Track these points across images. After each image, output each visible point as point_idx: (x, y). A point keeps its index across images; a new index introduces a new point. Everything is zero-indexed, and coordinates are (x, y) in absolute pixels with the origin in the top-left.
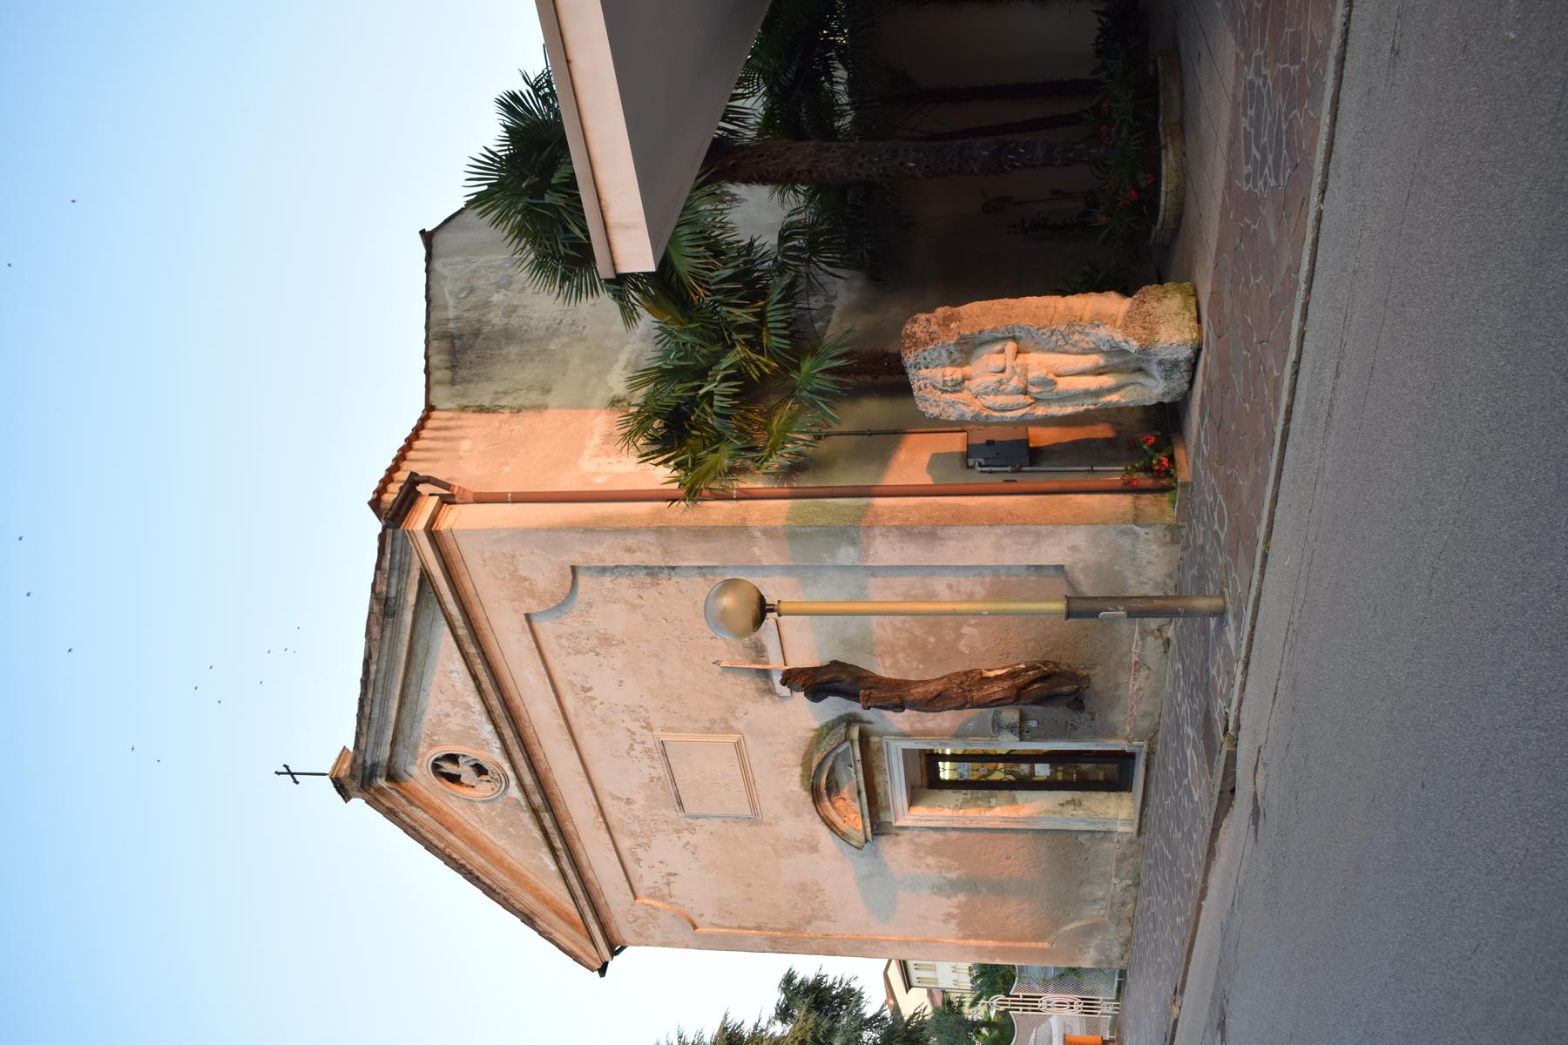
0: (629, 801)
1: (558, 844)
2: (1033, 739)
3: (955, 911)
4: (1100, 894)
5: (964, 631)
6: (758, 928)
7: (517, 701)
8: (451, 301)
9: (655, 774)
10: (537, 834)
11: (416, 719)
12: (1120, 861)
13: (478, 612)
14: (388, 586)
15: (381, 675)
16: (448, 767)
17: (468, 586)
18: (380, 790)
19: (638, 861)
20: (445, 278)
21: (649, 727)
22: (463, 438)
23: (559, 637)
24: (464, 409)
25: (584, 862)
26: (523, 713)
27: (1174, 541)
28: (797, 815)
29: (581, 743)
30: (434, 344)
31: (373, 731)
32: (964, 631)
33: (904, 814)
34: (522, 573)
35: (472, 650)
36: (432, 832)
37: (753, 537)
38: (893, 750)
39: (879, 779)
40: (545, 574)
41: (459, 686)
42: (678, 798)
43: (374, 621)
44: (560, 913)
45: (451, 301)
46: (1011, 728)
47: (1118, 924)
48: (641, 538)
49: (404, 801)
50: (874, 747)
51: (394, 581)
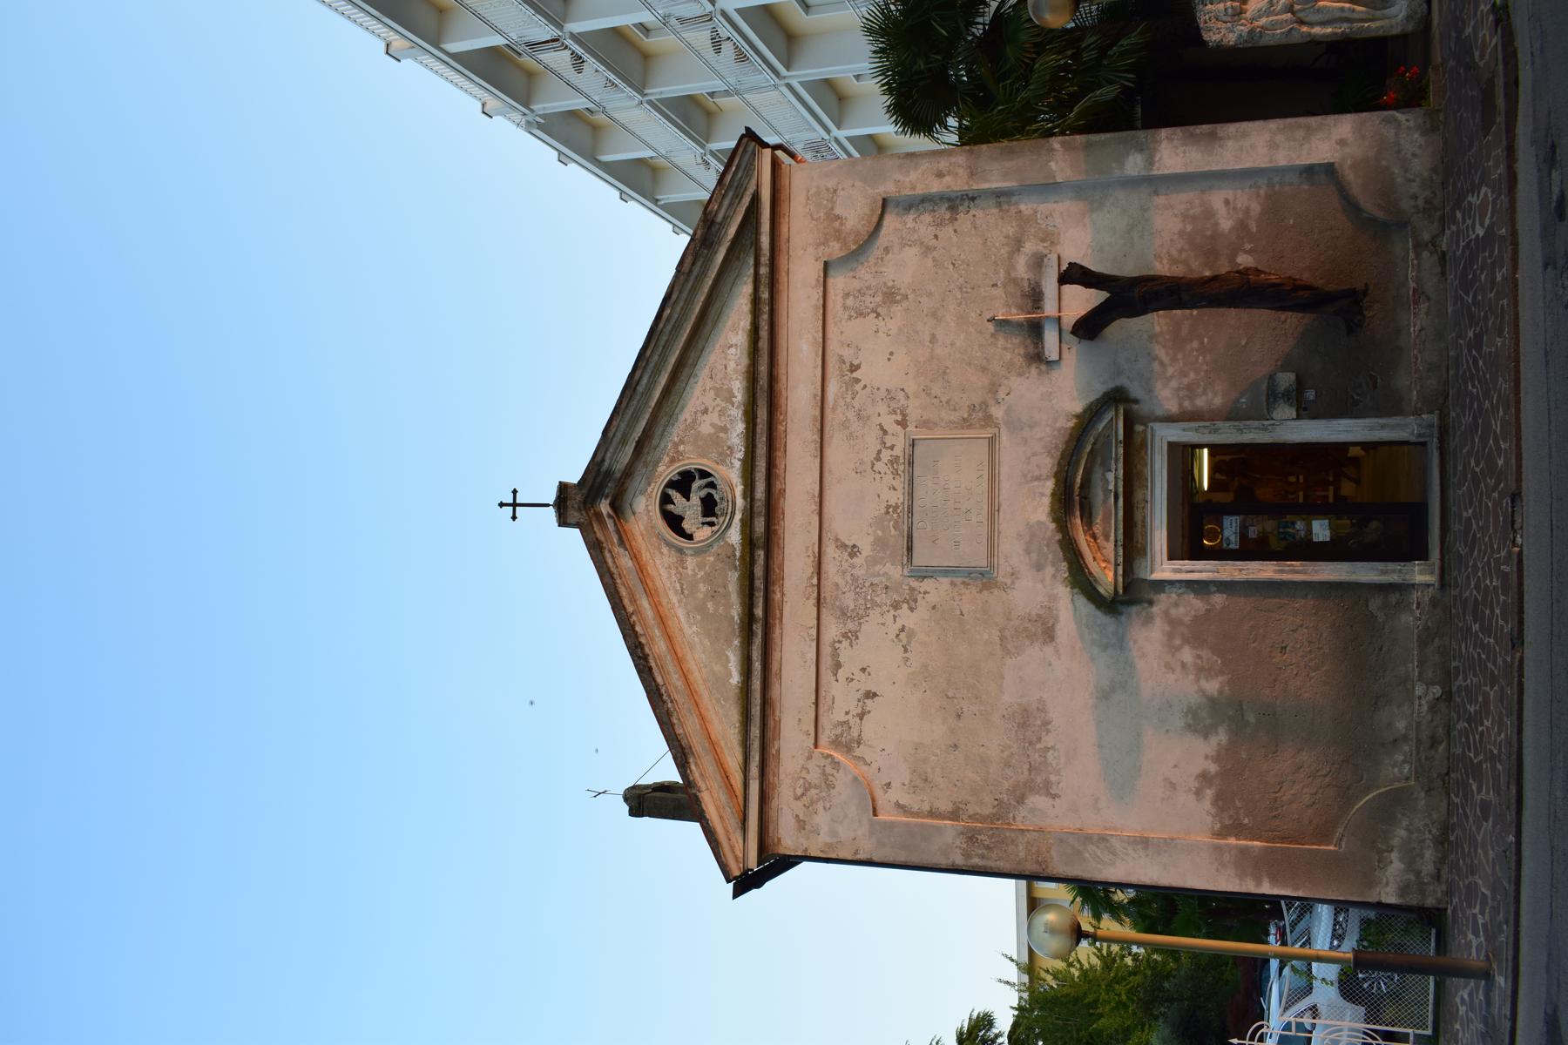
0: (854, 551)
3: (1213, 768)
4: (1401, 725)
6: (954, 815)
7: (782, 385)
10: (736, 612)
11: (672, 418)
12: (1423, 643)
15: (669, 328)
17: (784, 229)
18: (599, 515)
21: (903, 423)
23: (847, 295)
25: (775, 667)
26: (783, 401)
27: (1434, 129)
28: (1039, 567)
29: (828, 452)
33: (1163, 568)
34: (837, 211)
35: (765, 295)
36: (628, 588)
38: (1157, 439)
39: (1138, 495)
40: (854, 211)
41: (732, 365)
42: (910, 538)
46: (1286, 396)
47: (1429, 791)
50: (1138, 440)
51: (726, 202)
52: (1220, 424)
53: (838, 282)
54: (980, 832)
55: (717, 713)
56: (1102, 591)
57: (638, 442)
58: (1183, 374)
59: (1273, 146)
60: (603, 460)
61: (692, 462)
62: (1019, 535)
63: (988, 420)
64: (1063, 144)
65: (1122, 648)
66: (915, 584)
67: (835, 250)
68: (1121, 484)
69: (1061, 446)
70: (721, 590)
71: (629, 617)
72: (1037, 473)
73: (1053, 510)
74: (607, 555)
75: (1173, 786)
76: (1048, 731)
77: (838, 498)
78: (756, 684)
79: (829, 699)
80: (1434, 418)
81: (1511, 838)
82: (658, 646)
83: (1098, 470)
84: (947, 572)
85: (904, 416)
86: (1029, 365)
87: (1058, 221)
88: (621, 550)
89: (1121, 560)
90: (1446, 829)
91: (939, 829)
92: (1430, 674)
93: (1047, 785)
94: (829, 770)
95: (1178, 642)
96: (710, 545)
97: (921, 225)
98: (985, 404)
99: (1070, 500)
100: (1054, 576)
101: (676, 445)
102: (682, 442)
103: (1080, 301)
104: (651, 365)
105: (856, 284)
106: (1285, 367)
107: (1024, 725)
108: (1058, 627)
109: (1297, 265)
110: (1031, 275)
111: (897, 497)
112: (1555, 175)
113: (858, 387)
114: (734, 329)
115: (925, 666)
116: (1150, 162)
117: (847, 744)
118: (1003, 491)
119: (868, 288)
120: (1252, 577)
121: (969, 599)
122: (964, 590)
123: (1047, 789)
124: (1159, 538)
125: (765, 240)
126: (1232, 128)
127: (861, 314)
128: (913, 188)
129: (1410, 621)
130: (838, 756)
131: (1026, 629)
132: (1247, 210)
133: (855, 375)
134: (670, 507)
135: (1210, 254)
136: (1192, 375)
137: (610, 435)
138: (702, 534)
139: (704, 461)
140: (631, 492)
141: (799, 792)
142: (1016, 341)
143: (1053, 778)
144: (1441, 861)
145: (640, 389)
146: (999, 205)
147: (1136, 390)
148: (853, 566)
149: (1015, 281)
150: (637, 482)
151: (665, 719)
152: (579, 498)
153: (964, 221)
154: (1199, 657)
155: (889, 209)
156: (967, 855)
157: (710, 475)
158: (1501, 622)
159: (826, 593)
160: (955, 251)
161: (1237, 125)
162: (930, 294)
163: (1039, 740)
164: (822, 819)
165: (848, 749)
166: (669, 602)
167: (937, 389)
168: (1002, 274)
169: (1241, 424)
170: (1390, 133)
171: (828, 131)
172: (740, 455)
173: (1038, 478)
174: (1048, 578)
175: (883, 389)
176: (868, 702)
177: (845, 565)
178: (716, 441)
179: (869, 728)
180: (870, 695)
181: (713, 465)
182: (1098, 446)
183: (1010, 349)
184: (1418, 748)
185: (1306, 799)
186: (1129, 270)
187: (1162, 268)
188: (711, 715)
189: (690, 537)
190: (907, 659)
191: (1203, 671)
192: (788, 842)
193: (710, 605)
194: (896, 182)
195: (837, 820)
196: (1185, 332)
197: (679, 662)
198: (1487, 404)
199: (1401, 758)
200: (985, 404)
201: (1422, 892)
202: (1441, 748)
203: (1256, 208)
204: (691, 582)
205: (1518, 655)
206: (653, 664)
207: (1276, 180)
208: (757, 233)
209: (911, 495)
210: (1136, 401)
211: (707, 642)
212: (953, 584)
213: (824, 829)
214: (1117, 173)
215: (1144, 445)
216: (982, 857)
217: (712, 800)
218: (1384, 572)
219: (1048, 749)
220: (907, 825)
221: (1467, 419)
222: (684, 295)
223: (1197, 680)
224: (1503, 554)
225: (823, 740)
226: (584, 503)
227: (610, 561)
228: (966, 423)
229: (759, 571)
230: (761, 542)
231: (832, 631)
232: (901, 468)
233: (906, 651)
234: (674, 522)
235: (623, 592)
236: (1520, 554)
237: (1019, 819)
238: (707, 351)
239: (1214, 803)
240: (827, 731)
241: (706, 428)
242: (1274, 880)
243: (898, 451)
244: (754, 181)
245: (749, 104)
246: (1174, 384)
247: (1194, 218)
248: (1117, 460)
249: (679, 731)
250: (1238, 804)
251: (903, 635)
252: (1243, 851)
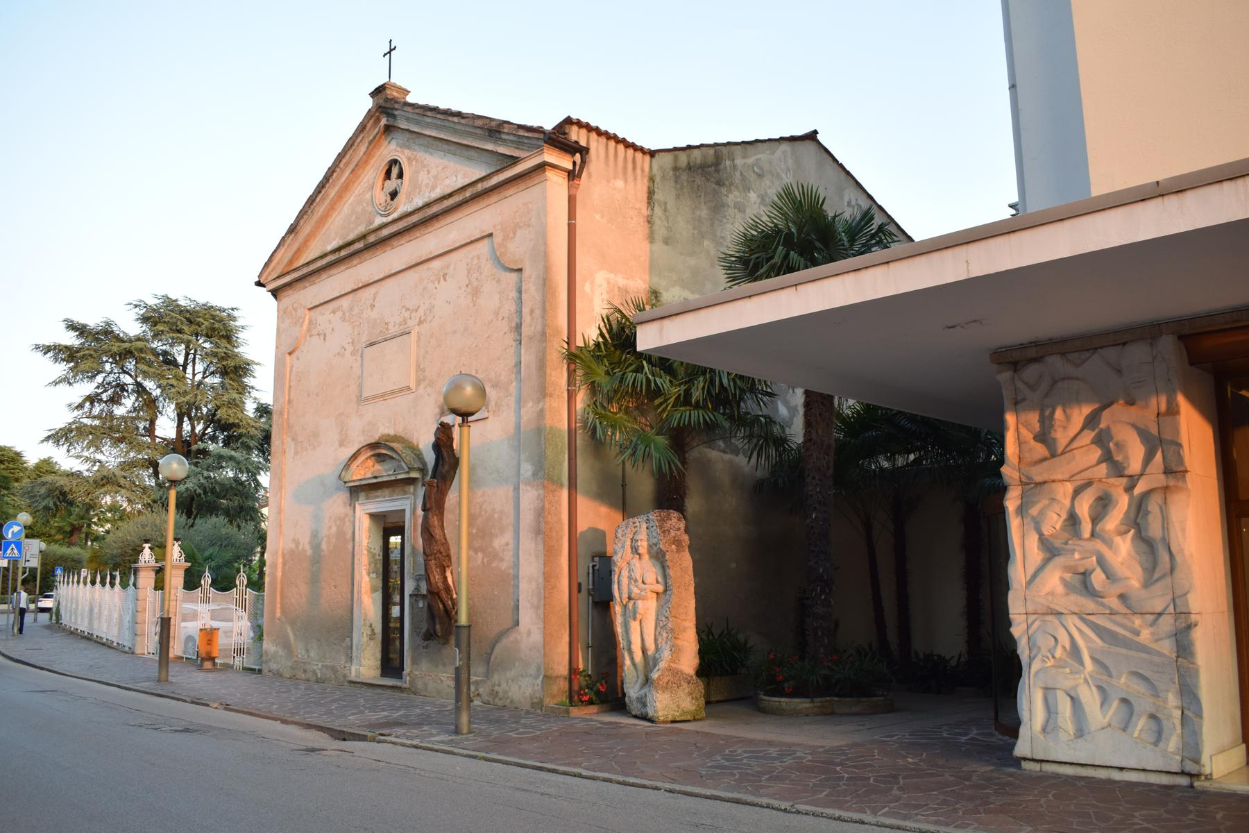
0: (373, 306)
1: (343, 253)
2: (411, 605)
4: (312, 654)
5: (480, 554)
6: (290, 401)
7: (437, 225)
8: (750, 161)
9: (390, 326)
10: (351, 237)
11: (427, 148)
13: (494, 198)
16: (395, 171)
17: (510, 192)
18: (378, 120)
19: (334, 312)
20: (773, 153)
21: (420, 323)
22: (626, 181)
24: (652, 179)
26: (430, 229)
27: (533, 705)
30: (711, 151)
32: (480, 554)
33: (364, 509)
35: (468, 194)
39: (387, 491)
40: (518, 249)
41: (447, 182)
43: (485, 121)
44: (299, 252)
45: (750, 161)
47: (292, 668)
50: (407, 488)
51: (511, 138)
116: (528, 483)
132: (502, 560)
235: (347, 157)
247: (501, 519)
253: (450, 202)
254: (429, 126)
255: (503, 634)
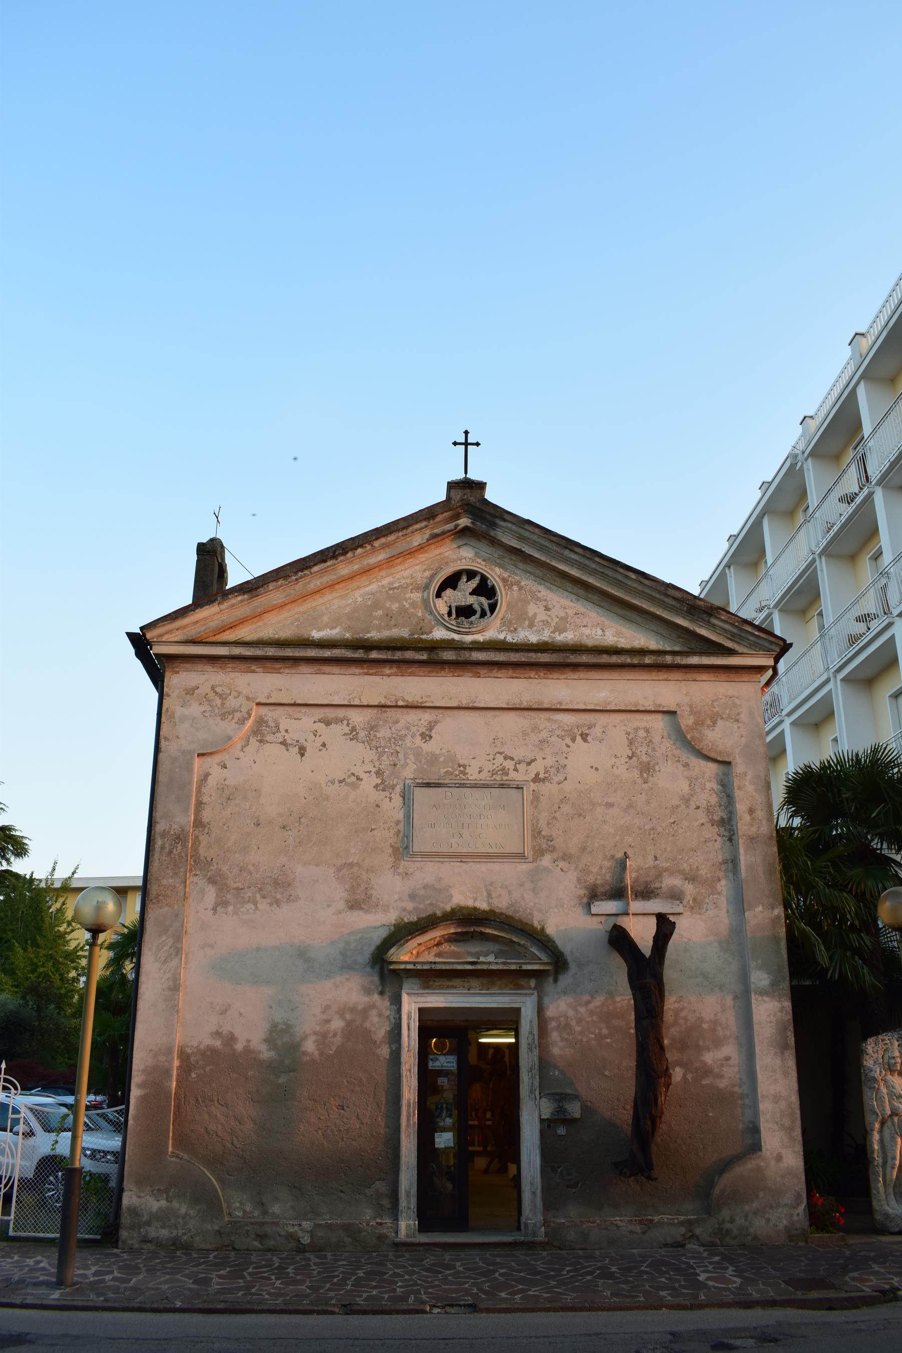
0: (426, 737)
3: (239, 1047)
5: (678, 1069)
6: (199, 823)
7: (570, 675)
10: (374, 635)
11: (542, 580)
14: (723, 621)
15: (619, 577)
17: (704, 677)
18: (457, 517)
21: (537, 779)
23: (647, 731)
25: (326, 669)
26: (556, 675)
28: (412, 897)
29: (512, 715)
31: (547, 544)
33: (412, 1003)
34: (720, 723)
35: (647, 660)
36: (395, 542)
37: (773, 909)
39: (474, 982)
40: (721, 737)
41: (587, 631)
42: (438, 785)
44: (242, 622)
46: (560, 1110)
47: (219, 1232)
48: (764, 822)
49: (436, 531)
50: (523, 982)
51: (727, 627)
52: (536, 1052)
53: (659, 724)
54: (184, 846)
55: (286, 619)
56: (392, 950)
57: (520, 550)
58: (579, 1021)
59: (776, 1098)
60: (505, 520)
61: (504, 597)
62: (440, 879)
63: (539, 853)
64: (778, 917)
65: (342, 968)
66: (398, 789)
67: (687, 721)
68: (485, 967)
69: (517, 916)
70: (393, 622)
71: (370, 542)
72: (494, 895)
73: (461, 908)
74: (423, 524)
75: (223, 1012)
76: (271, 904)
77: (472, 723)
78: (312, 653)
79: (299, 715)
80: (541, 1236)
81: (178, 1304)
82: (344, 568)
83: (495, 947)
84: (408, 817)
85: (543, 780)
86: (586, 888)
87: (711, 913)
88: (427, 536)
89: (419, 967)
90: (187, 1248)
91: (187, 809)
92: (320, 1233)
93: (225, 904)
94: (238, 715)
95: (348, 1016)
96: (431, 613)
97: (708, 795)
98: (553, 850)
99: (471, 924)
100: (404, 910)
101: (518, 583)
102: (521, 588)
103: (642, 932)
104: (587, 562)
105: (657, 739)
106: (585, 1109)
107: (276, 883)
108: (361, 913)
109: (673, 1119)
110: (664, 890)
111: (473, 775)
112: (751, 1342)
113: (568, 741)
114: (618, 634)
115: (327, 798)
116: (762, 993)
117: (260, 731)
118: (478, 866)
119: (654, 749)
120: (404, 1080)
121: (385, 836)
122: (392, 832)
123: (221, 903)
124: (437, 1000)
125: (695, 660)
126: (792, 1063)
127: (631, 743)
128: (739, 788)
129: (366, 1217)
130: (250, 723)
131: (359, 885)
132: (720, 1076)
133: (579, 738)
134: (464, 578)
135: (682, 1045)
136: (578, 1029)
137: (527, 527)
138: (441, 606)
139: (504, 608)
140: (478, 544)
141: (219, 690)
142: (608, 877)
143: (231, 908)
144: (159, 1244)
145: (567, 553)
146: (725, 862)
147: (565, 980)
148: (413, 736)
149: (659, 876)
150: (486, 549)
151: (282, 574)
152: (472, 499)
153: (712, 832)
154: (335, 1035)
155: (721, 767)
156: (164, 834)
157: (492, 612)
158: (365, 1295)
159: (390, 713)
160: (685, 824)
161: (794, 1068)
162: (648, 802)
163: (264, 897)
164: (195, 709)
165: (256, 732)
166: (383, 578)
167: (566, 808)
168: (666, 865)
169: (536, 1071)
170: (788, 1199)
171: (789, 714)
172: (509, 639)
173: (489, 895)
174: (403, 904)
175: (566, 762)
176: (296, 749)
177: (414, 729)
178: (521, 618)
179: (273, 750)
180: (302, 751)
181: (501, 616)
182: (517, 947)
183: (600, 871)
184: (257, 1223)
185: (212, 1127)
186: (670, 974)
187: (671, 1003)
188: (285, 614)
189: (438, 595)
190: (333, 782)
191: (323, 1038)
192: (175, 680)
193: (380, 612)
194: (745, 774)
195: (195, 723)
196: (616, 1022)
197: (331, 586)
198: (553, 1283)
199: (248, 1209)
200: (553, 850)
201: (132, 1227)
202: (257, 1244)
203: (722, 1084)
204: (399, 598)
205: (337, 1310)
206: (328, 563)
207: (747, 1101)
208: (701, 653)
209: (475, 786)
210: (556, 980)
211: (348, 610)
212: (398, 822)
213: (186, 711)
214: (753, 964)
215: (519, 987)
216: (162, 848)
217: (212, 615)
218: (408, 1194)
219: (255, 904)
220: (190, 783)
221: (540, 1266)
222: (647, 591)
223: (315, 1033)
224: (424, 1297)
225: (264, 710)
226: (468, 504)
227: (418, 526)
228: (537, 833)
229: (409, 655)
230: (434, 657)
231: (358, 718)
232: (498, 778)
233: (340, 782)
234: (451, 582)
235: (391, 538)
236: (423, 1312)
237: (195, 879)
238: (600, 610)
239: (209, 1048)
240: (270, 714)
241: (532, 609)
242: (143, 1099)
243: (513, 775)
244: (745, 650)
245: (812, 646)
246: (571, 1013)
247: (714, 1030)
248: (505, 963)
249: (271, 586)
250: (208, 1069)
251: (354, 779)
252: (167, 1073)
253: (614, 659)
254: (567, 560)
255: (726, 1165)
